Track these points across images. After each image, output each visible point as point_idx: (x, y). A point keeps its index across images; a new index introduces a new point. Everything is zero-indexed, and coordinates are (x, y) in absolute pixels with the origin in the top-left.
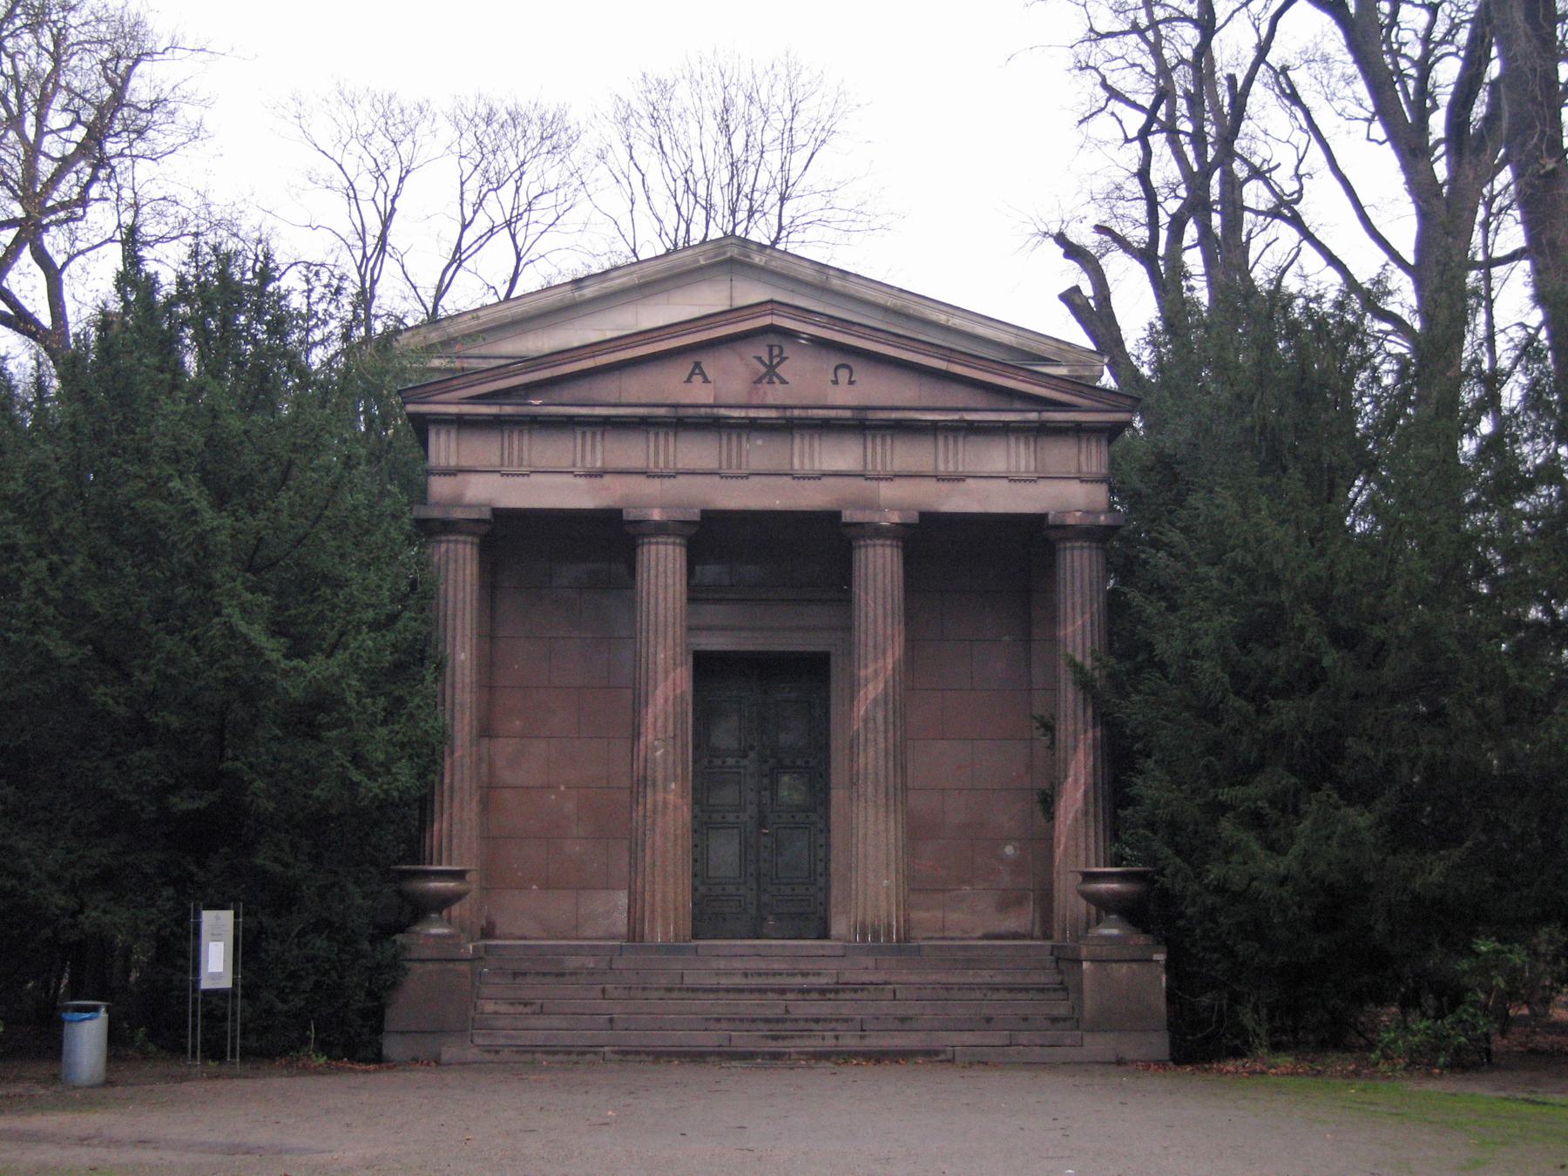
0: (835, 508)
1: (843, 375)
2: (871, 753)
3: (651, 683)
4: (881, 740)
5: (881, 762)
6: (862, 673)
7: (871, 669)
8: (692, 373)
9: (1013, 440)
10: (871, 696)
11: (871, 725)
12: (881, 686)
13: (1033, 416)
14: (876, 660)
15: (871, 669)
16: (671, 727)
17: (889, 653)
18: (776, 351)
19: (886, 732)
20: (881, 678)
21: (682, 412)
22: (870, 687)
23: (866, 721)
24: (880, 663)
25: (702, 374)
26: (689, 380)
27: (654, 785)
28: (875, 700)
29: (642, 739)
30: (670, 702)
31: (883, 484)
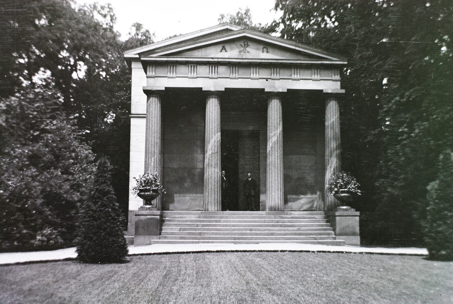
0: (263, 87)
1: (265, 50)
2: (273, 157)
3: (211, 137)
4: (276, 154)
5: (276, 160)
6: (271, 134)
7: (273, 134)
8: (222, 49)
9: (313, 70)
10: (273, 141)
11: (273, 149)
12: (276, 138)
13: (320, 62)
14: (275, 131)
15: (273, 134)
16: (216, 150)
17: (279, 129)
18: (246, 43)
19: (278, 151)
20: (276, 136)
21: (220, 60)
22: (273, 138)
23: (272, 148)
24: (276, 132)
25: (225, 49)
26: (221, 51)
27: (211, 165)
28: (274, 142)
29: (208, 153)
30: (216, 142)
31: (276, 81)
